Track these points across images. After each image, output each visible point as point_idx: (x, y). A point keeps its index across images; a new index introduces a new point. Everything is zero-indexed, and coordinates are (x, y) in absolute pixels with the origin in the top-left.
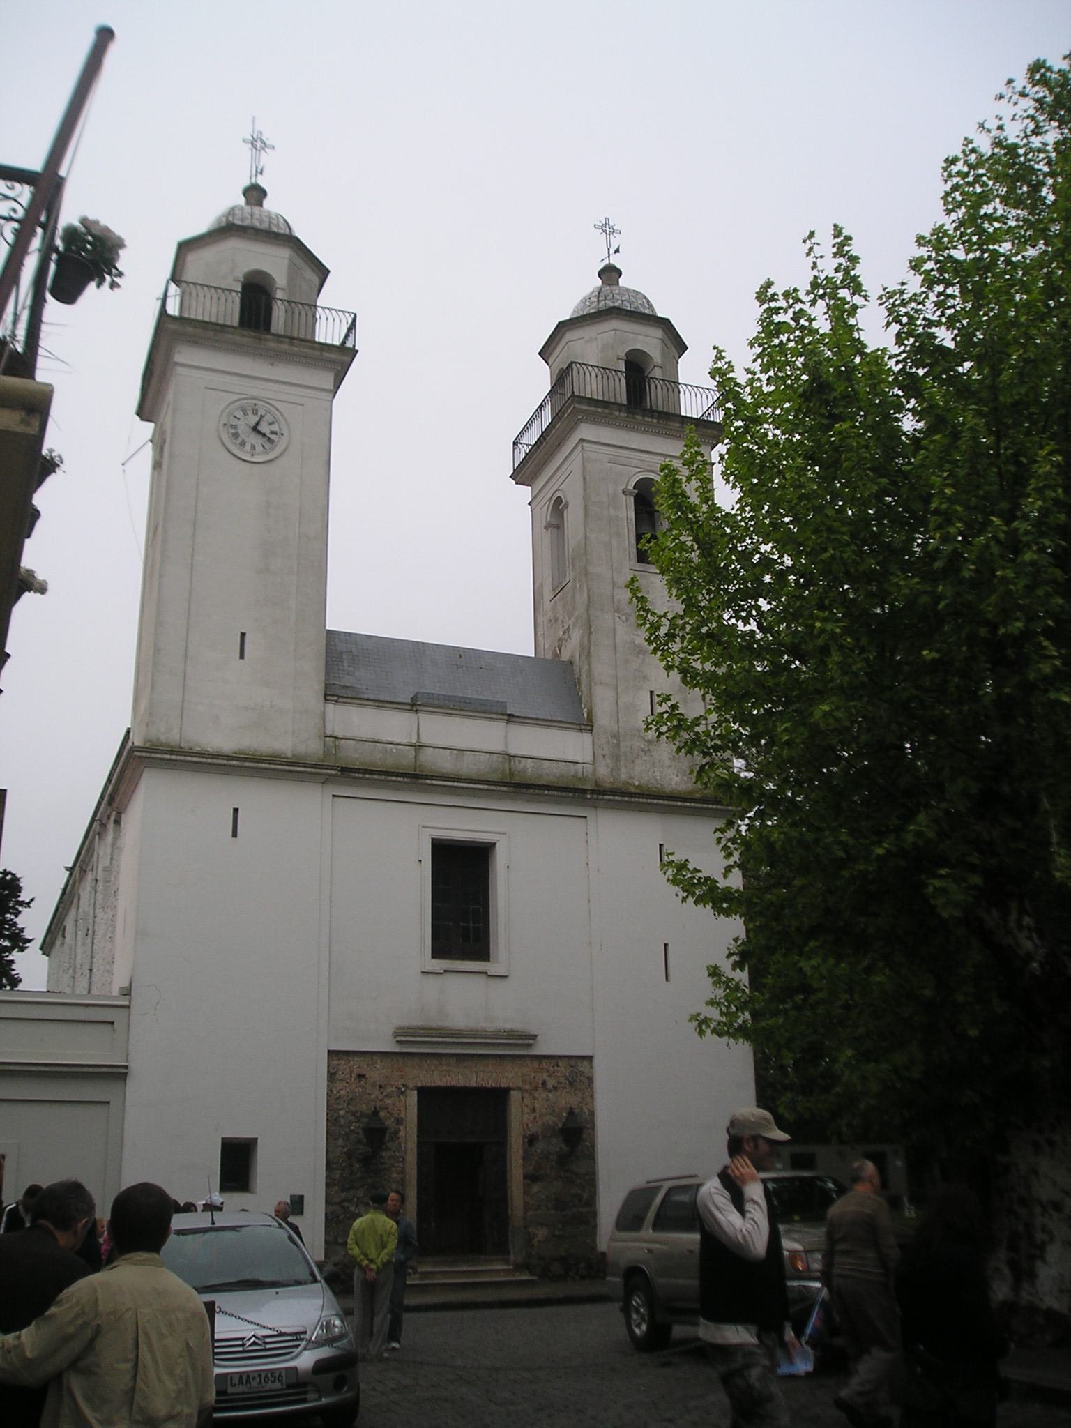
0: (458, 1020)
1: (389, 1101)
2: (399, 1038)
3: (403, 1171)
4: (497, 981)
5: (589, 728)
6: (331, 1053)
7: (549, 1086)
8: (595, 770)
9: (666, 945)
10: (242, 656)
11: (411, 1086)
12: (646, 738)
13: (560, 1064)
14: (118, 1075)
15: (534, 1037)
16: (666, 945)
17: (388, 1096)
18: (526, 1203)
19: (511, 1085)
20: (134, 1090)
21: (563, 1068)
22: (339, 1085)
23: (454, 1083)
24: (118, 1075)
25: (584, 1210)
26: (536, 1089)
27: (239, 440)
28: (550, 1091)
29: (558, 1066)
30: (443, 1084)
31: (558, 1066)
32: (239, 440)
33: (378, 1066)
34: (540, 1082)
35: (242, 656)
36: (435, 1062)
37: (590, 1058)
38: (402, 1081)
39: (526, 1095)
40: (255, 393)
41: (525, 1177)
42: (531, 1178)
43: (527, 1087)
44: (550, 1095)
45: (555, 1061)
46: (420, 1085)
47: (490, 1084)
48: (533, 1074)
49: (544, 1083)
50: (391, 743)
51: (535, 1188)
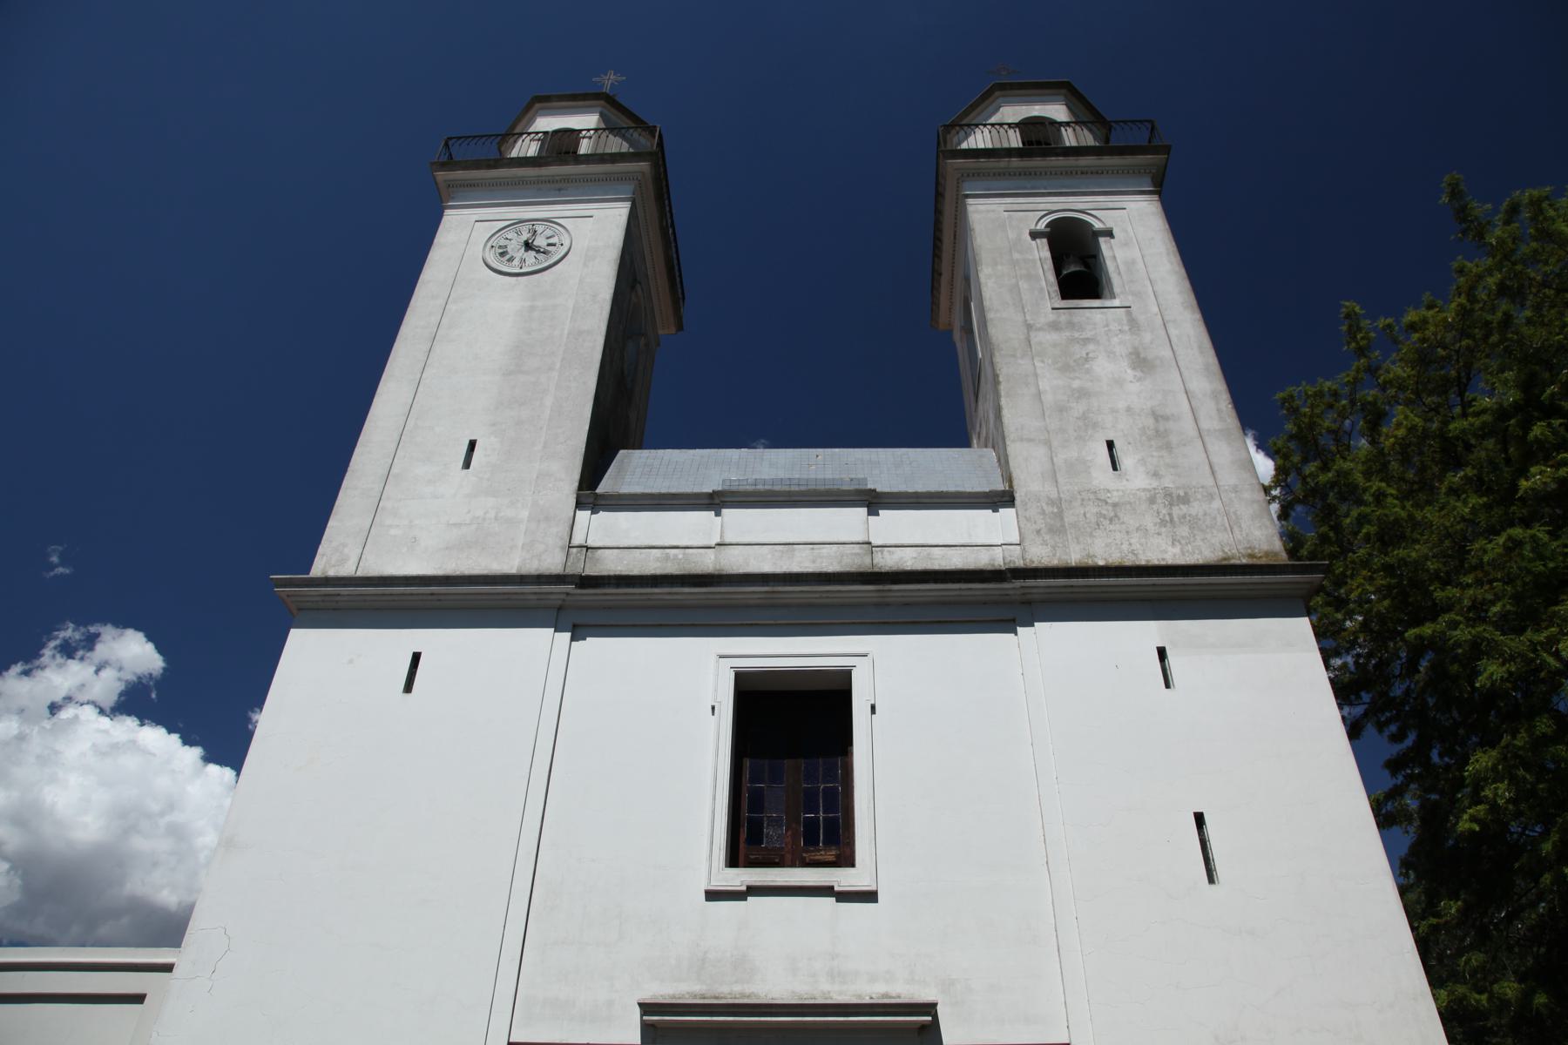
8: (1024, 551)
9: (1199, 819)
10: (467, 465)
12: (1109, 501)
16: (1199, 819)
27: (508, 257)
32: (508, 257)
35: (467, 465)
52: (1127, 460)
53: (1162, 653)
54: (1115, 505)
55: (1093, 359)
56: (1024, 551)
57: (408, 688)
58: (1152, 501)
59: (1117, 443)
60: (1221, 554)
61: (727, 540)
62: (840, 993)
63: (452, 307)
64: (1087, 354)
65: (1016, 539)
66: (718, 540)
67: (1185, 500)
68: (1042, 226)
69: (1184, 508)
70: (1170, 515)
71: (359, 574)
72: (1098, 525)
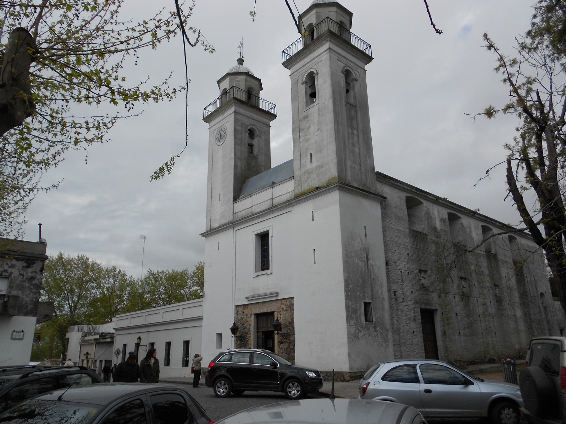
0: (261, 291)
1: (248, 319)
2: (249, 299)
3: (251, 341)
4: (270, 275)
5: (292, 178)
6: (237, 306)
7: (284, 310)
9: (314, 249)
11: (252, 314)
14: (200, 319)
15: (277, 293)
17: (248, 318)
18: (278, 351)
19: (275, 311)
20: (204, 322)
21: (288, 302)
22: (239, 315)
23: (261, 312)
24: (200, 319)
25: (294, 354)
28: (284, 311)
30: (259, 312)
36: (258, 305)
37: (293, 298)
39: (278, 313)
40: (220, 126)
41: (279, 342)
42: (280, 343)
43: (279, 310)
49: (283, 309)
51: (282, 346)
52: (313, 159)
53: (313, 211)
55: (310, 127)
57: (219, 250)
58: (316, 169)
63: (214, 159)
67: (322, 167)
68: (304, 81)
69: (322, 169)
70: (319, 172)
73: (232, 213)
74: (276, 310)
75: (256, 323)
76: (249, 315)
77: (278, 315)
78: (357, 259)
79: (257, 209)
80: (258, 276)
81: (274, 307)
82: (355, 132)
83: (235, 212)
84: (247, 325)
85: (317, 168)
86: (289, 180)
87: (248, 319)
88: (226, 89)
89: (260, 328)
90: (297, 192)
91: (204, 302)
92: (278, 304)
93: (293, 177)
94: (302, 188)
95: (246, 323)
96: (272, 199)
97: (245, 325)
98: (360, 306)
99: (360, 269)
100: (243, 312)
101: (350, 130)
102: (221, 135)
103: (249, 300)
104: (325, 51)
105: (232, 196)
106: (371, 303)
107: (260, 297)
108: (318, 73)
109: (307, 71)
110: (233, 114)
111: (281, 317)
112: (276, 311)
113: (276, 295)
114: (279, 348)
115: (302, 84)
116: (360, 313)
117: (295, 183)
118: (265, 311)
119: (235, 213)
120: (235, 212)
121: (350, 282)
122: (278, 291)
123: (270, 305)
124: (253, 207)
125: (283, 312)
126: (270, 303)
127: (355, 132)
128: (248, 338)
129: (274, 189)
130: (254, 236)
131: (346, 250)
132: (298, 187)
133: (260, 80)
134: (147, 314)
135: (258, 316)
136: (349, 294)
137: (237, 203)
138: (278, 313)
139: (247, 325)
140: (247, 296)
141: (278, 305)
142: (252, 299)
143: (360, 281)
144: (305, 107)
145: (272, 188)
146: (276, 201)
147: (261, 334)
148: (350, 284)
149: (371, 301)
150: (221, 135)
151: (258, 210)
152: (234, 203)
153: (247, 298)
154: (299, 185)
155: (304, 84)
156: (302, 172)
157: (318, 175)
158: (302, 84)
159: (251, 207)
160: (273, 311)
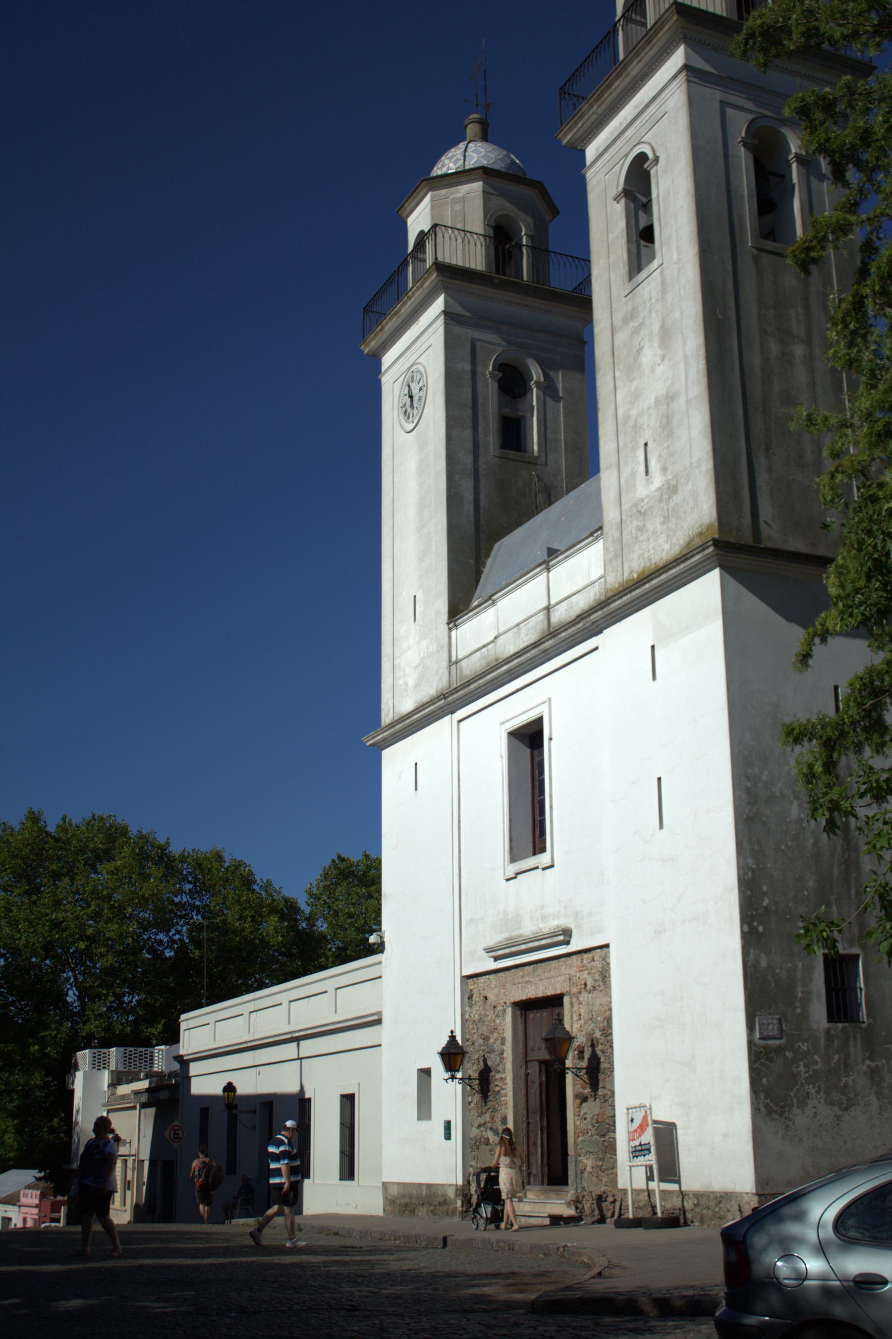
1: (498, 1021)
2: (494, 954)
3: (506, 1096)
5: (599, 532)
7: (588, 987)
11: (508, 1002)
12: (643, 511)
13: (595, 959)
15: (567, 934)
18: (576, 1127)
19: (564, 991)
20: (385, 1033)
26: (580, 993)
28: (590, 992)
29: (593, 960)
31: (593, 960)
33: (492, 986)
34: (583, 982)
37: (607, 946)
38: (504, 1001)
41: (576, 1096)
44: (590, 995)
45: (589, 955)
46: (512, 1001)
47: (550, 992)
48: (578, 975)
49: (585, 985)
50: (484, 646)
52: (653, 463)
53: (653, 647)
54: (645, 513)
56: (605, 581)
59: (649, 444)
60: (688, 539)
61: (501, 631)
62: (545, 928)
63: (396, 479)
64: (640, 344)
65: (600, 572)
66: (495, 634)
69: (674, 497)
70: (668, 509)
71: (395, 718)
72: (636, 539)
73: (445, 664)
74: (568, 989)
75: (521, 1034)
76: (499, 1008)
77: (572, 1004)
78: (799, 805)
79: (509, 646)
80: (519, 876)
81: (562, 979)
82: (799, 351)
83: (454, 659)
84: (496, 1040)
85: (662, 495)
86: (590, 539)
87: (498, 1021)
88: (422, 232)
89: (533, 1050)
90: (614, 581)
91: (383, 964)
92: (572, 967)
93: (601, 528)
94: (626, 566)
95: (492, 1032)
96: (548, 609)
97: (492, 1040)
98: (809, 970)
99: (811, 841)
100: (486, 998)
101: (774, 348)
102: (411, 397)
103: (496, 959)
104: (675, 77)
105: (442, 605)
106: (857, 957)
107: (523, 947)
108: (657, 159)
109: (627, 155)
110: (441, 321)
111: (582, 1011)
112: (569, 993)
113: (561, 938)
114: (577, 1115)
115: (616, 199)
116: (807, 994)
117: (606, 549)
118: (540, 994)
119: (453, 663)
120: (454, 659)
121: (765, 888)
122: (569, 923)
123: (552, 973)
124: (500, 641)
125: (584, 996)
126: (554, 963)
127: (799, 351)
128: (500, 1084)
129: (552, 573)
130: (504, 737)
131: (748, 778)
132: (614, 563)
133: (541, 184)
134: (251, 1006)
135: (525, 1007)
136: (761, 929)
137: (460, 629)
138: (574, 1000)
139: (496, 1040)
140: (490, 943)
141: (572, 973)
142: (507, 951)
143: (811, 884)
144: (626, 277)
145: (548, 570)
146: (560, 615)
147: (534, 1069)
148: (765, 894)
149: (855, 950)
150: (411, 397)
151: (512, 649)
152: (450, 629)
153: (489, 950)
154: (616, 557)
155: (623, 201)
156: (624, 508)
157: (666, 519)
158: (616, 199)
159: (493, 642)
160: (559, 992)
